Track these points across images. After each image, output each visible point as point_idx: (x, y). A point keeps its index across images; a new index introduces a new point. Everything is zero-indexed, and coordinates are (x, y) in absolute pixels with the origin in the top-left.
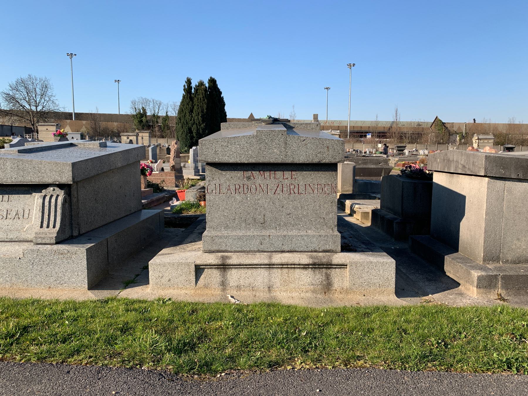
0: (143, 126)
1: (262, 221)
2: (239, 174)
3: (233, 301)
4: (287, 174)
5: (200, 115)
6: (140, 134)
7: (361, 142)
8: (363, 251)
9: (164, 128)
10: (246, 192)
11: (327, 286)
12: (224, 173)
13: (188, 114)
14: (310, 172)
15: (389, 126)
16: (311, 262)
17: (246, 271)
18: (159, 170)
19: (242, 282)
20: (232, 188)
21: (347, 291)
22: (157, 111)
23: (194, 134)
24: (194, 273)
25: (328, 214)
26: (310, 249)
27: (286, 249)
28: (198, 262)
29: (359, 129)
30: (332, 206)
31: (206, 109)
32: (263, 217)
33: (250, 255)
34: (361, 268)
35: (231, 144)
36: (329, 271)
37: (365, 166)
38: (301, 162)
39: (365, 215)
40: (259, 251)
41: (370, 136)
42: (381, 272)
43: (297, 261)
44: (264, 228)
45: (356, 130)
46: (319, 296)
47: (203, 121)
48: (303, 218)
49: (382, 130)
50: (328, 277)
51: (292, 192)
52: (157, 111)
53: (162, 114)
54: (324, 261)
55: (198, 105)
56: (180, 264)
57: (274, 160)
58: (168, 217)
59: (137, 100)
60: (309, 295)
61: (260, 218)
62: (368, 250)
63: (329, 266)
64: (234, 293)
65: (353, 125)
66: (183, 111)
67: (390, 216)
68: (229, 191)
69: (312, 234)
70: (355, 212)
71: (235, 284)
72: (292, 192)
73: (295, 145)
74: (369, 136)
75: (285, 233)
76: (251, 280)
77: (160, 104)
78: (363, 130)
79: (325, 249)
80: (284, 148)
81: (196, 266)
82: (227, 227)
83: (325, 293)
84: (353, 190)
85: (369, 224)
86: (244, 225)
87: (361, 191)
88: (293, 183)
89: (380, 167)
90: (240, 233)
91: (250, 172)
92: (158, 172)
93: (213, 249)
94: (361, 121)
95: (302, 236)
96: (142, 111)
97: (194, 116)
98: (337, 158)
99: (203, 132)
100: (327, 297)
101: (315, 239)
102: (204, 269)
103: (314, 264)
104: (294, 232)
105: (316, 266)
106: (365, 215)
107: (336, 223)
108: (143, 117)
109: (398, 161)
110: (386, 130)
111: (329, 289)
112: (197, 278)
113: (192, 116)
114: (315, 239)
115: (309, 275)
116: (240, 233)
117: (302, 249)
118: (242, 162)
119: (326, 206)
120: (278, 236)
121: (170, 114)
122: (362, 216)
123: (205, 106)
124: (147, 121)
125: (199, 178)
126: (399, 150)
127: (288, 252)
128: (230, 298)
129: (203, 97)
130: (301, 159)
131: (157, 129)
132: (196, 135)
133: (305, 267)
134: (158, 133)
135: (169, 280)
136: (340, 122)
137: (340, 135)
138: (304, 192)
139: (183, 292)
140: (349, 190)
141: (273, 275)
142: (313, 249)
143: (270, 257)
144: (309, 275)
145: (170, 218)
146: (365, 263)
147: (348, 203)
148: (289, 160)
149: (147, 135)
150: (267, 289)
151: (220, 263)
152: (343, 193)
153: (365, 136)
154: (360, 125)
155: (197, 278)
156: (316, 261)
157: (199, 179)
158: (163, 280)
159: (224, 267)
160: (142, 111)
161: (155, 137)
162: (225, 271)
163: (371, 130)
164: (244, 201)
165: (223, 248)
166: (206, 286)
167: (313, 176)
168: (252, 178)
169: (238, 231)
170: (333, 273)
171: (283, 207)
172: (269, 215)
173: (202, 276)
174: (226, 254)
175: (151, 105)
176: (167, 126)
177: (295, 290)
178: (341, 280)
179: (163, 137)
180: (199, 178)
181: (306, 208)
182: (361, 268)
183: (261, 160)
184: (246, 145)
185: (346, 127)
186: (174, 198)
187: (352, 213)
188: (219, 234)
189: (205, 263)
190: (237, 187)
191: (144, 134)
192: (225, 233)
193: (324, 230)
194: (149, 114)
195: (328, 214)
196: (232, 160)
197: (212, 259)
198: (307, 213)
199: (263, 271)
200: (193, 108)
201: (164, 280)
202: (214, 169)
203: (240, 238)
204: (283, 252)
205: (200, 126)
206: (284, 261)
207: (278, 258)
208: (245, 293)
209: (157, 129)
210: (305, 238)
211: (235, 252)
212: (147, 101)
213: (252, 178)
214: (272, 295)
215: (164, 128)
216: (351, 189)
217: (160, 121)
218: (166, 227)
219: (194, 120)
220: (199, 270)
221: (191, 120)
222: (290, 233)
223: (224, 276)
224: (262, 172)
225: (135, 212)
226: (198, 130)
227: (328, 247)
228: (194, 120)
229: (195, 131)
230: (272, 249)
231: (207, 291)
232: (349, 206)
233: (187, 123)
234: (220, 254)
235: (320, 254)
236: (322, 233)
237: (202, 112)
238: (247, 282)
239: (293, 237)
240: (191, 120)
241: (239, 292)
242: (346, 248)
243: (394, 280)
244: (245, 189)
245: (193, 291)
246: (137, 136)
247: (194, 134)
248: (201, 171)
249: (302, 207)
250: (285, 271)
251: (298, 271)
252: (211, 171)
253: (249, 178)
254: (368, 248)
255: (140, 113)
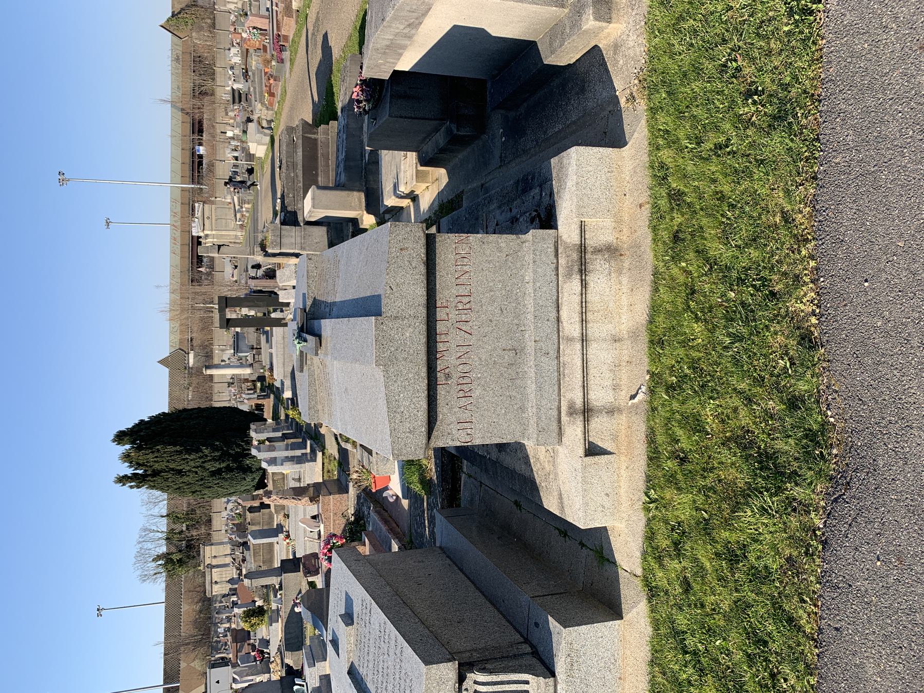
0: (188, 557)
1: (512, 354)
2: (441, 391)
3: (640, 396)
4: (440, 314)
5: (187, 456)
6: (208, 561)
7: (211, 165)
8: (551, 194)
9: (192, 519)
10: (468, 381)
11: (611, 251)
12: (440, 417)
13: (185, 479)
14: (438, 277)
15: (180, 113)
16: (578, 277)
17: (591, 377)
18: (316, 524)
19: (609, 383)
20: (463, 402)
21: (619, 221)
22: (160, 535)
23: (223, 465)
24: (597, 458)
25: (500, 250)
26: (554, 278)
27: (553, 315)
28: (581, 452)
29: (188, 168)
30: (488, 243)
31: (175, 445)
32: (506, 352)
33: (566, 371)
34: (586, 199)
35: (399, 407)
36: (589, 249)
37: (300, 167)
38: (425, 293)
39: (420, 177)
40: (558, 357)
41: (201, 148)
42: (591, 169)
43: (577, 299)
44: (523, 349)
45: (188, 173)
46: (626, 265)
47: (198, 450)
48: (508, 289)
49: (188, 127)
50: (598, 251)
51: (468, 306)
52: (160, 535)
53: (163, 525)
54: (575, 256)
55: (168, 461)
56: (585, 481)
57: (422, 337)
58: (442, 503)
59: (139, 572)
60: (625, 280)
61: (508, 357)
62: (547, 185)
63: (582, 249)
64: (624, 394)
65: (179, 179)
66: (179, 488)
67: (440, 138)
68: (468, 407)
69: (531, 274)
70: (413, 191)
71: (611, 392)
72: (468, 306)
73: (398, 303)
74: (202, 150)
75: (530, 317)
76: (605, 368)
77: (145, 530)
78: (188, 160)
79: (553, 253)
80: (403, 320)
81: (586, 456)
82: (522, 409)
83: (621, 255)
84: (359, 191)
85: (443, 171)
86: (518, 382)
87: (362, 175)
88: (454, 305)
89: (300, 141)
90: (532, 388)
91: (439, 374)
92: (322, 526)
93: (556, 431)
94: (172, 163)
95: (535, 290)
96: (160, 562)
97: (188, 468)
98: (418, 234)
99: (218, 450)
100: (627, 253)
101: (539, 270)
102: (589, 442)
103: (581, 271)
104: (529, 302)
105: (583, 271)
106: (420, 177)
107: (514, 237)
108: (171, 559)
109: (263, 104)
110: (188, 119)
111: (616, 250)
112: (604, 452)
113: (189, 471)
114: (539, 270)
115: (596, 279)
116: (532, 388)
117: (554, 290)
118: (426, 388)
119: (488, 253)
120: (536, 327)
121: (164, 512)
122: (423, 181)
123: (170, 448)
124: (180, 551)
125: (319, 455)
126: (240, 101)
127: (558, 311)
128: (636, 400)
129: (153, 452)
130: (421, 292)
131: (194, 533)
132: (223, 461)
133: (584, 285)
134: (203, 530)
135: (607, 495)
136: (173, 201)
137: (204, 202)
138: (468, 288)
139: (623, 473)
140: (358, 198)
141: (597, 335)
142: (554, 273)
143: (570, 340)
144: (596, 279)
145: (443, 500)
146: (578, 193)
147: (390, 201)
148: (423, 311)
149: (208, 548)
150: (618, 344)
151: (582, 418)
152: (364, 208)
153: (201, 157)
154: (179, 165)
155: (604, 452)
156: (576, 268)
157: (323, 454)
158: (607, 505)
159: (587, 412)
160: (160, 562)
161: (209, 534)
162: (592, 410)
163: (189, 146)
164: (483, 383)
165: (555, 413)
166: (615, 438)
167: (444, 273)
168: (447, 371)
169: (529, 391)
170: (591, 243)
171: (491, 321)
172: (503, 343)
173: (600, 444)
174: (564, 409)
175: (149, 545)
176: (188, 514)
177: (620, 303)
178: (602, 232)
179: (210, 521)
180: (319, 455)
181: (491, 284)
182: (586, 199)
183: (422, 357)
184: (399, 383)
185: (183, 190)
186: (384, 495)
187: (414, 197)
188: (532, 422)
189: (582, 441)
190: (461, 394)
191: (207, 554)
192: (531, 411)
193: (524, 256)
194: (164, 549)
195: (500, 250)
196: (424, 405)
197: (574, 431)
198: (500, 281)
199: (590, 351)
200: (173, 469)
201: (607, 503)
202: (435, 433)
203: (540, 388)
204: (558, 319)
205: (207, 456)
206: (577, 318)
207: (571, 327)
208: (624, 377)
209: (194, 533)
210: (538, 285)
211: (559, 395)
212: (141, 554)
213: (447, 371)
214: (626, 336)
215: (192, 519)
216: (355, 193)
217: (178, 527)
218: (459, 506)
219: (197, 467)
220: (592, 450)
221: (196, 473)
222: (531, 308)
223: (600, 411)
224: (438, 356)
225: (448, 557)
226: (214, 459)
227: (551, 250)
228: (197, 467)
229: (217, 465)
230: (555, 337)
231: (622, 437)
232: (397, 200)
233: (202, 479)
234: (564, 418)
235: (562, 261)
236: (529, 258)
237: (180, 452)
238: (608, 375)
239: (536, 304)
240: (196, 473)
241: (623, 387)
242: (548, 220)
243: (601, 149)
244: (464, 382)
245: (623, 458)
246: (211, 567)
247: (223, 465)
248: (304, 451)
249: (491, 291)
250: (590, 316)
251: (590, 297)
252: (437, 438)
253: (448, 376)
254: (540, 186)
255: (165, 565)
